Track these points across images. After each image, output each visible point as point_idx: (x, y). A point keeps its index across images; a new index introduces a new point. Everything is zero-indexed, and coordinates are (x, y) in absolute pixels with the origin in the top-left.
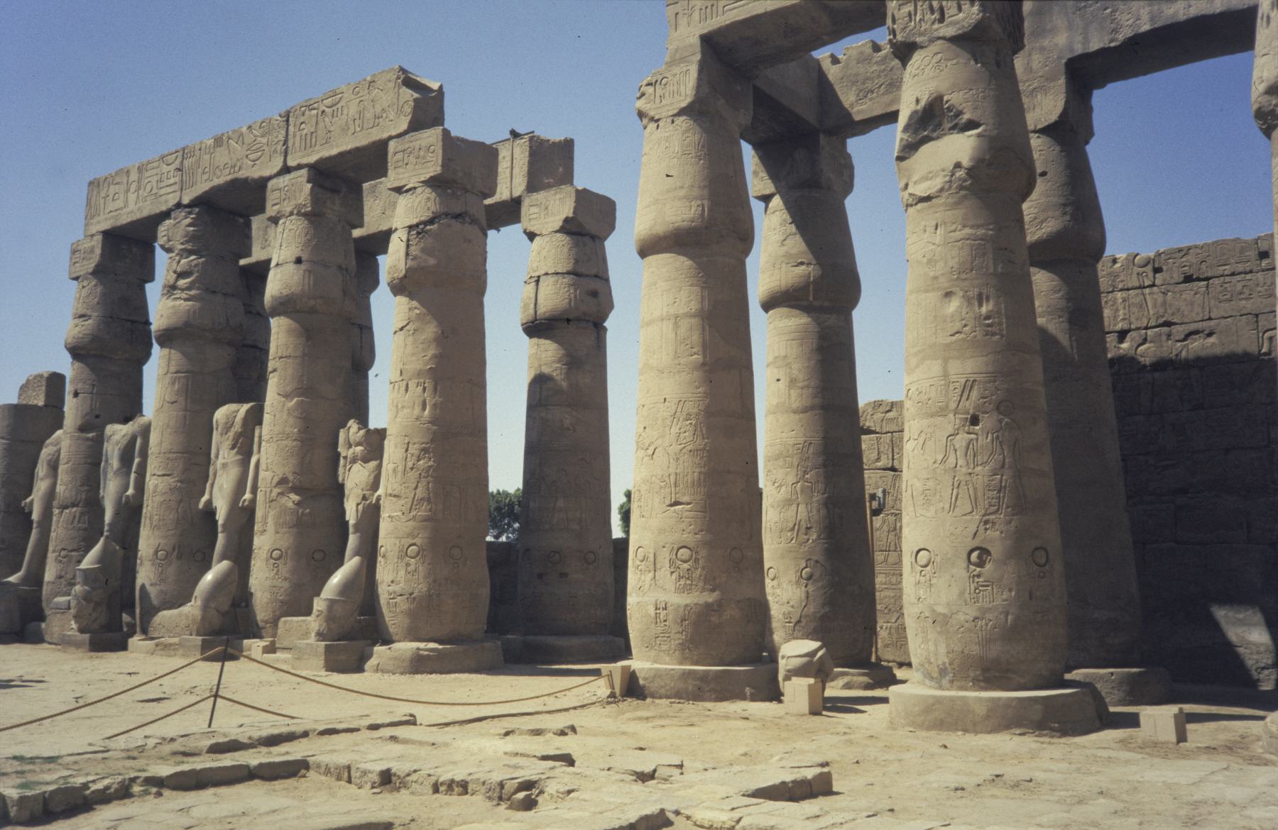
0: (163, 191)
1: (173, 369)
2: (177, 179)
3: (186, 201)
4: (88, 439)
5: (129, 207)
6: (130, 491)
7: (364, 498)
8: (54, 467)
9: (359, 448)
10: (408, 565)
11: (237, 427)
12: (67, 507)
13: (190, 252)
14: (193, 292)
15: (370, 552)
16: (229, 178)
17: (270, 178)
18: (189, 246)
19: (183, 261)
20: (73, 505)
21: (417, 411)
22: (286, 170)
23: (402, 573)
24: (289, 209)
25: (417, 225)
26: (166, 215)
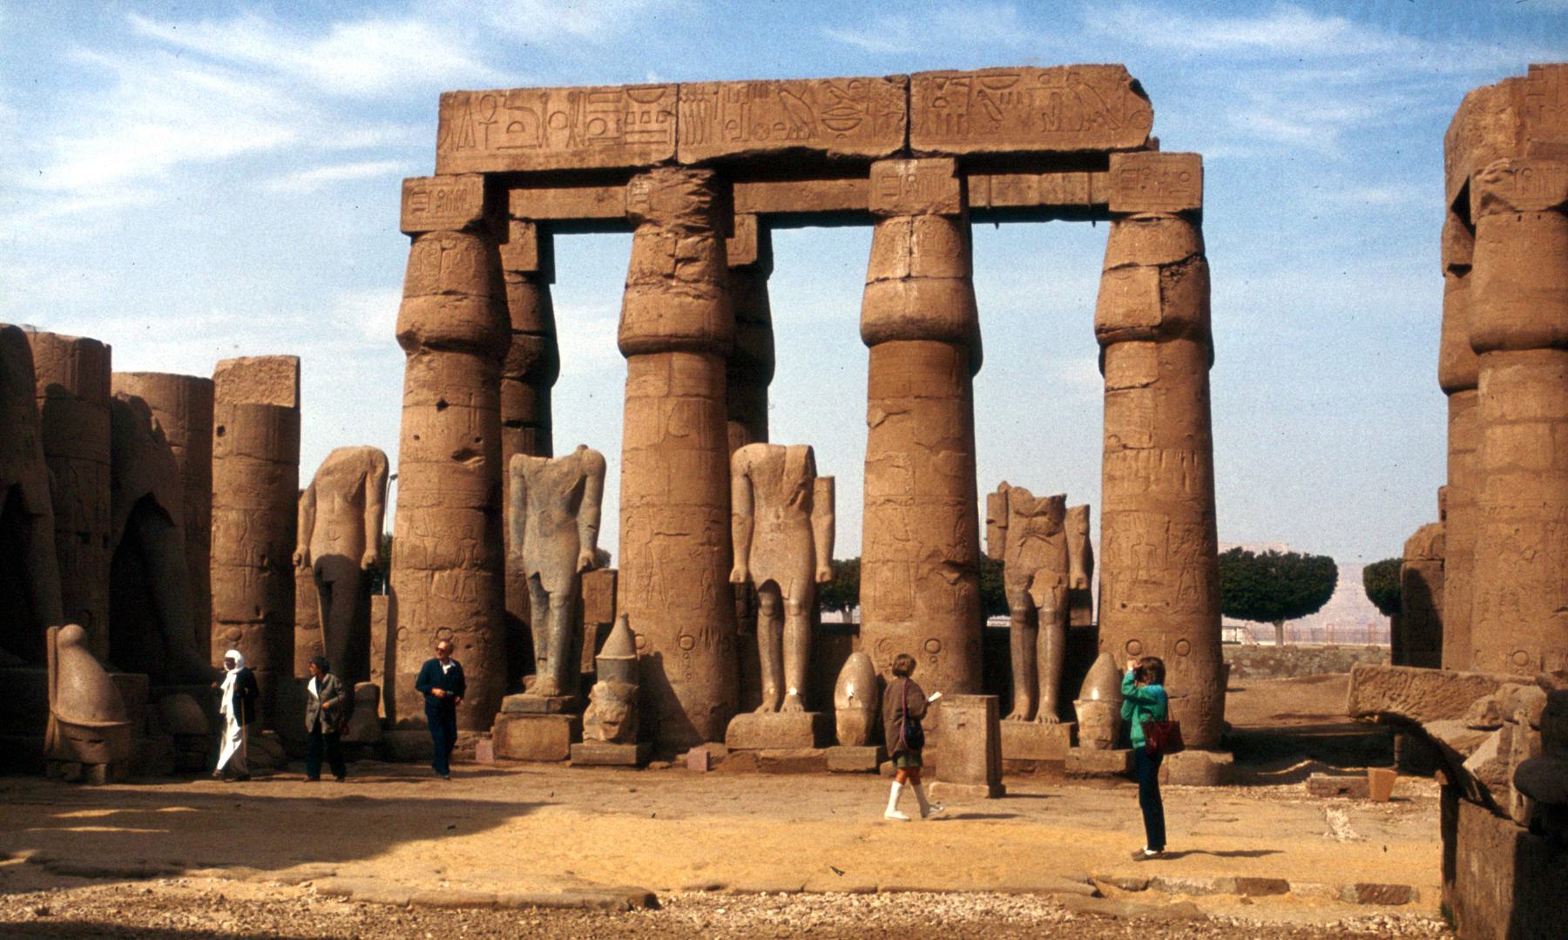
0: (629, 139)
1: (678, 390)
3: (687, 158)
4: (467, 472)
9: (1042, 520)
10: (1179, 663)
12: (441, 568)
13: (691, 231)
14: (702, 287)
16: (788, 144)
17: (877, 159)
19: (681, 243)
20: (453, 566)
21: (1177, 484)
22: (906, 153)
24: (918, 207)
25: (1170, 265)
26: (646, 170)
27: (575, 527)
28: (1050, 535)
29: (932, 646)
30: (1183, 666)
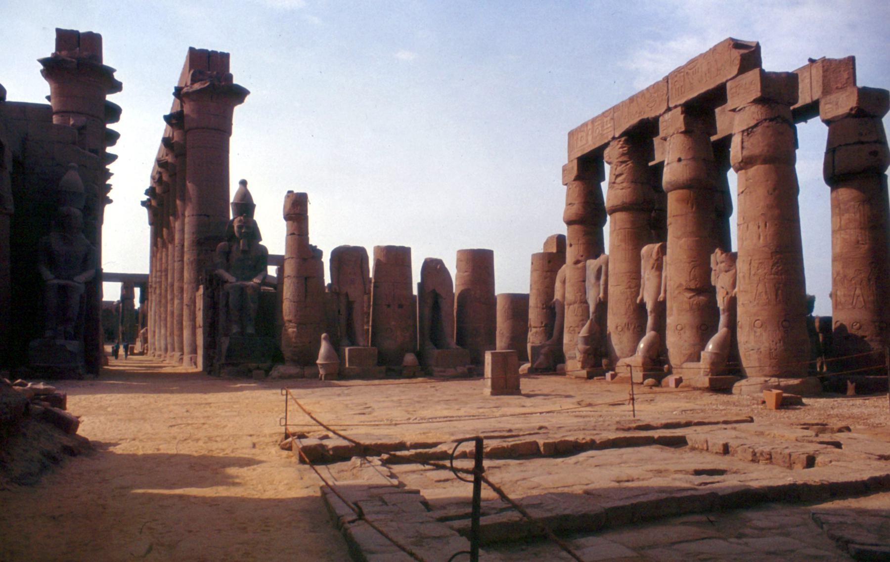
1: (617, 228)
2: (612, 124)
3: (617, 136)
4: (578, 269)
5: (588, 145)
6: (601, 295)
7: (727, 293)
8: (564, 282)
9: (723, 264)
11: (654, 256)
13: (622, 162)
14: (624, 185)
15: (732, 325)
17: (660, 115)
18: (620, 160)
20: (575, 303)
22: (669, 109)
23: (752, 337)
25: (747, 130)
26: (606, 145)
27: (599, 285)
28: (726, 272)
29: (679, 327)
30: (758, 334)
